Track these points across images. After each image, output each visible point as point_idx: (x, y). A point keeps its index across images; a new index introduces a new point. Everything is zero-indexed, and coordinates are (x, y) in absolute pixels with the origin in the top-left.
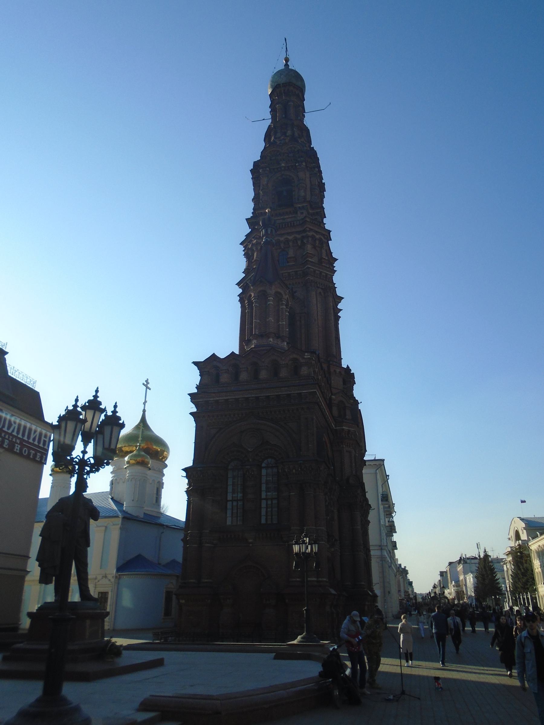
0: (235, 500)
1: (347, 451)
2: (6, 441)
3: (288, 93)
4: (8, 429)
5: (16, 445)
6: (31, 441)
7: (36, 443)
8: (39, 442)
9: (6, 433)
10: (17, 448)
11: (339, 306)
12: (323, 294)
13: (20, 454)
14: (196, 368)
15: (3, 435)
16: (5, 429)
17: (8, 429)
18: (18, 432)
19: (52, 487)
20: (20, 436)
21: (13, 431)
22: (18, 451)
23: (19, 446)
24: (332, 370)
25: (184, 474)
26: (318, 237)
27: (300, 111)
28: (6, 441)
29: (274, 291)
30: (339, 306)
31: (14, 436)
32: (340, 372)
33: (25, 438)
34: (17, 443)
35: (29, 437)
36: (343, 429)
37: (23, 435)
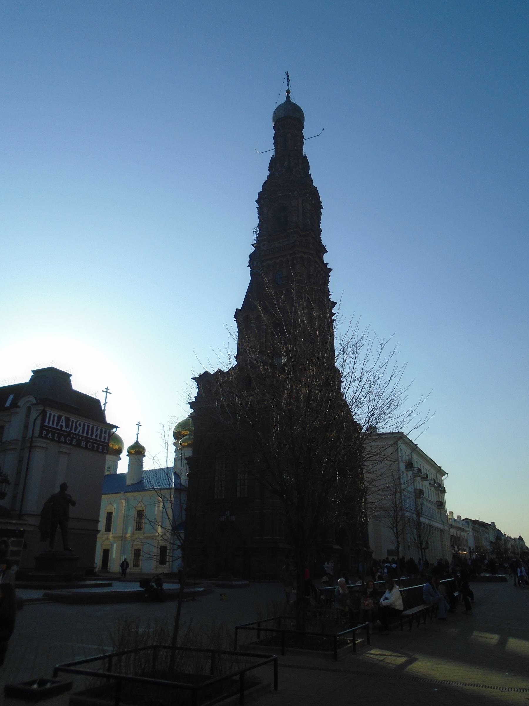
3: (289, 124)
4: (75, 430)
6: (94, 437)
7: (98, 438)
8: (100, 437)
9: (74, 434)
10: (83, 444)
11: (334, 311)
13: (86, 448)
15: (71, 436)
16: (73, 431)
17: (75, 430)
18: (83, 432)
19: (129, 465)
20: (85, 435)
21: (79, 432)
26: (306, 256)
27: (300, 140)
30: (334, 311)
31: (80, 436)
33: (89, 436)
35: (92, 434)
37: (87, 434)
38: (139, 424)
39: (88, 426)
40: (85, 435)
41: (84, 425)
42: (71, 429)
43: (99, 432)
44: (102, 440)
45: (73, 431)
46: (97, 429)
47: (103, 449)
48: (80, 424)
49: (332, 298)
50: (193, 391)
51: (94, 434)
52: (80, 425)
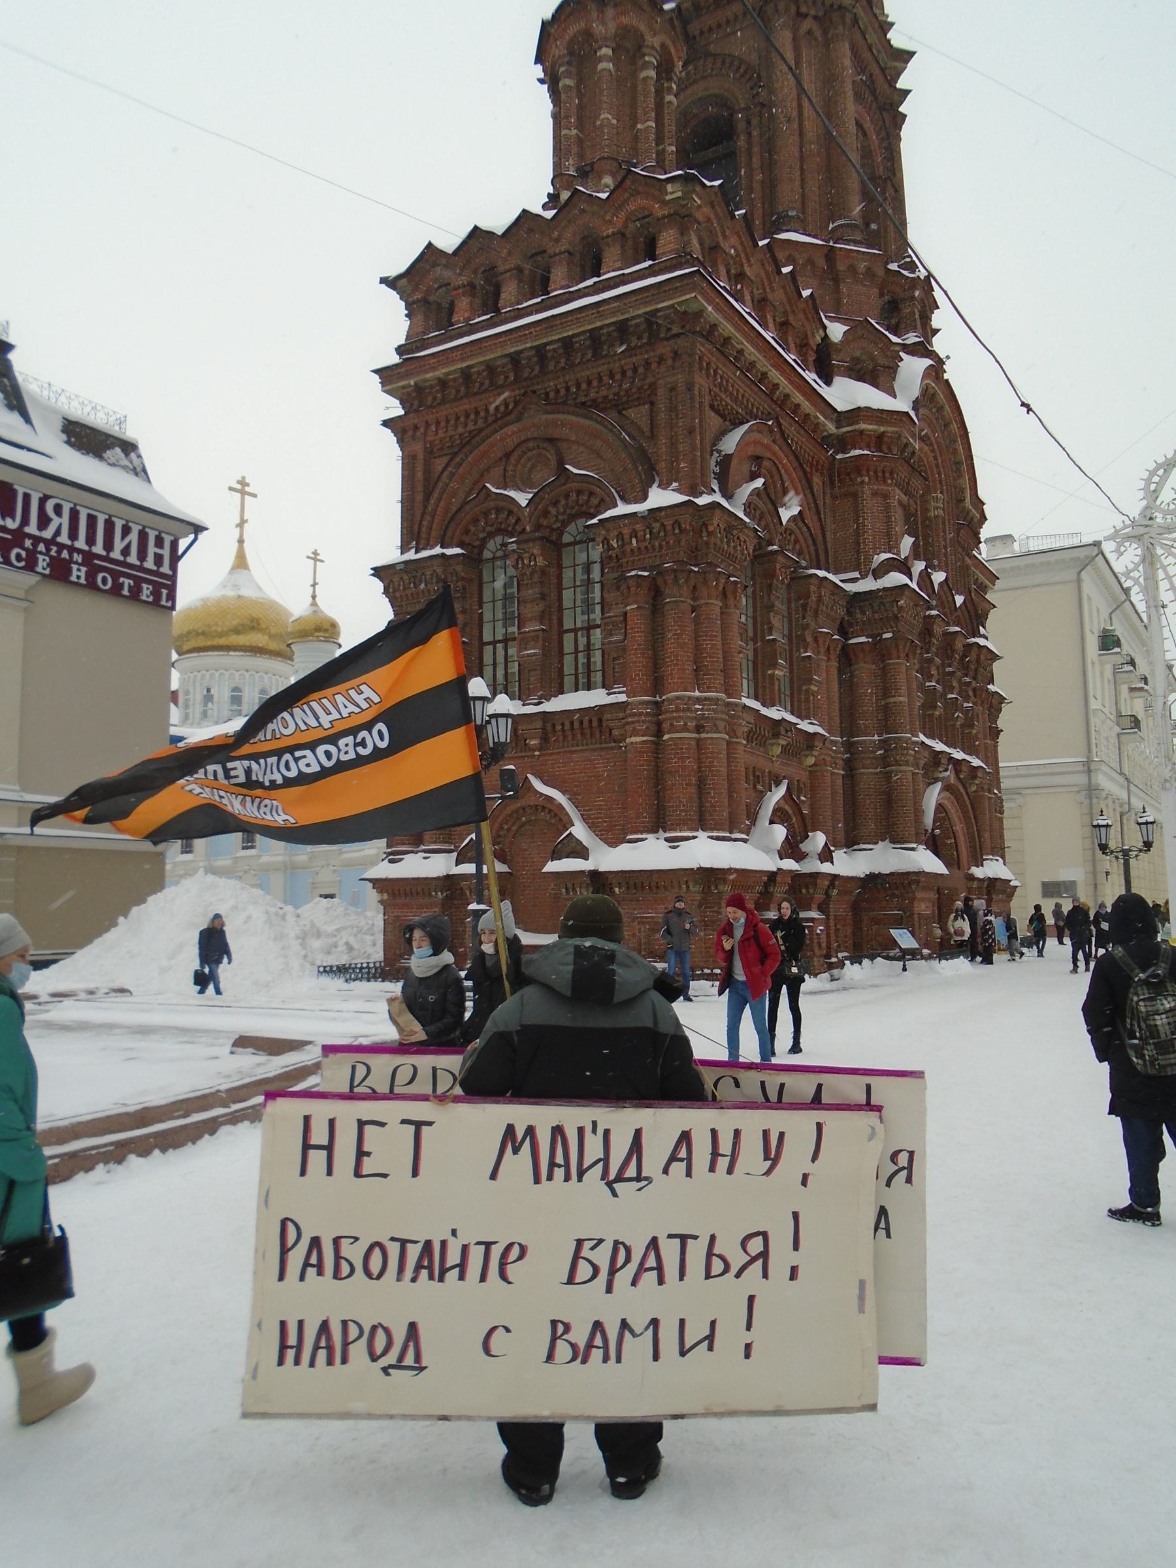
0: (500, 642)
1: (875, 494)
2: (41, 557)
5: (75, 567)
6: (116, 554)
7: (133, 559)
8: (142, 555)
9: (37, 540)
10: (79, 573)
12: (818, 34)
13: (91, 585)
14: (393, 295)
15: (28, 543)
16: (32, 529)
18: (73, 535)
20: (81, 544)
21: (58, 532)
22: (83, 581)
23: (84, 569)
24: (841, 267)
25: (379, 586)
28: (41, 557)
29: (612, 27)
30: (901, 84)
31: (61, 547)
32: (868, 269)
33: (99, 549)
34: (76, 563)
35: (109, 545)
36: (862, 432)
37: (91, 541)
38: (315, 557)
39: (92, 520)
40: (81, 544)
41: (74, 515)
42: (25, 521)
43: (133, 537)
44: (150, 564)
45: (32, 529)
46: (126, 530)
47: (156, 594)
48: (58, 509)
49: (897, 38)
50: (388, 325)
51: (119, 545)
52: (58, 509)
